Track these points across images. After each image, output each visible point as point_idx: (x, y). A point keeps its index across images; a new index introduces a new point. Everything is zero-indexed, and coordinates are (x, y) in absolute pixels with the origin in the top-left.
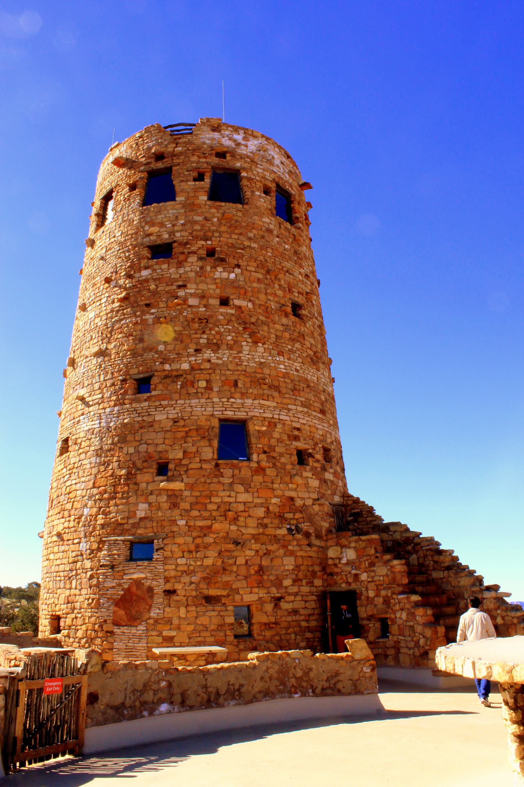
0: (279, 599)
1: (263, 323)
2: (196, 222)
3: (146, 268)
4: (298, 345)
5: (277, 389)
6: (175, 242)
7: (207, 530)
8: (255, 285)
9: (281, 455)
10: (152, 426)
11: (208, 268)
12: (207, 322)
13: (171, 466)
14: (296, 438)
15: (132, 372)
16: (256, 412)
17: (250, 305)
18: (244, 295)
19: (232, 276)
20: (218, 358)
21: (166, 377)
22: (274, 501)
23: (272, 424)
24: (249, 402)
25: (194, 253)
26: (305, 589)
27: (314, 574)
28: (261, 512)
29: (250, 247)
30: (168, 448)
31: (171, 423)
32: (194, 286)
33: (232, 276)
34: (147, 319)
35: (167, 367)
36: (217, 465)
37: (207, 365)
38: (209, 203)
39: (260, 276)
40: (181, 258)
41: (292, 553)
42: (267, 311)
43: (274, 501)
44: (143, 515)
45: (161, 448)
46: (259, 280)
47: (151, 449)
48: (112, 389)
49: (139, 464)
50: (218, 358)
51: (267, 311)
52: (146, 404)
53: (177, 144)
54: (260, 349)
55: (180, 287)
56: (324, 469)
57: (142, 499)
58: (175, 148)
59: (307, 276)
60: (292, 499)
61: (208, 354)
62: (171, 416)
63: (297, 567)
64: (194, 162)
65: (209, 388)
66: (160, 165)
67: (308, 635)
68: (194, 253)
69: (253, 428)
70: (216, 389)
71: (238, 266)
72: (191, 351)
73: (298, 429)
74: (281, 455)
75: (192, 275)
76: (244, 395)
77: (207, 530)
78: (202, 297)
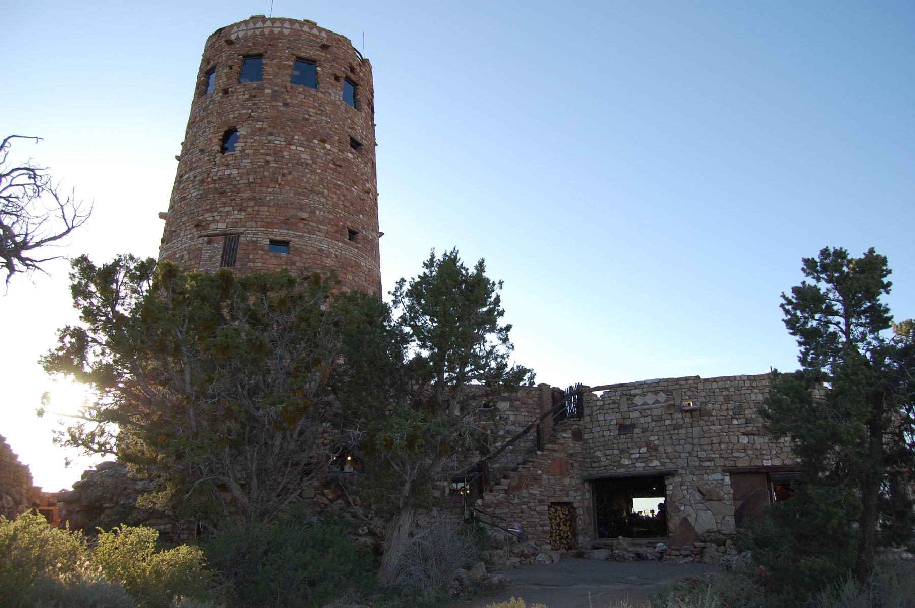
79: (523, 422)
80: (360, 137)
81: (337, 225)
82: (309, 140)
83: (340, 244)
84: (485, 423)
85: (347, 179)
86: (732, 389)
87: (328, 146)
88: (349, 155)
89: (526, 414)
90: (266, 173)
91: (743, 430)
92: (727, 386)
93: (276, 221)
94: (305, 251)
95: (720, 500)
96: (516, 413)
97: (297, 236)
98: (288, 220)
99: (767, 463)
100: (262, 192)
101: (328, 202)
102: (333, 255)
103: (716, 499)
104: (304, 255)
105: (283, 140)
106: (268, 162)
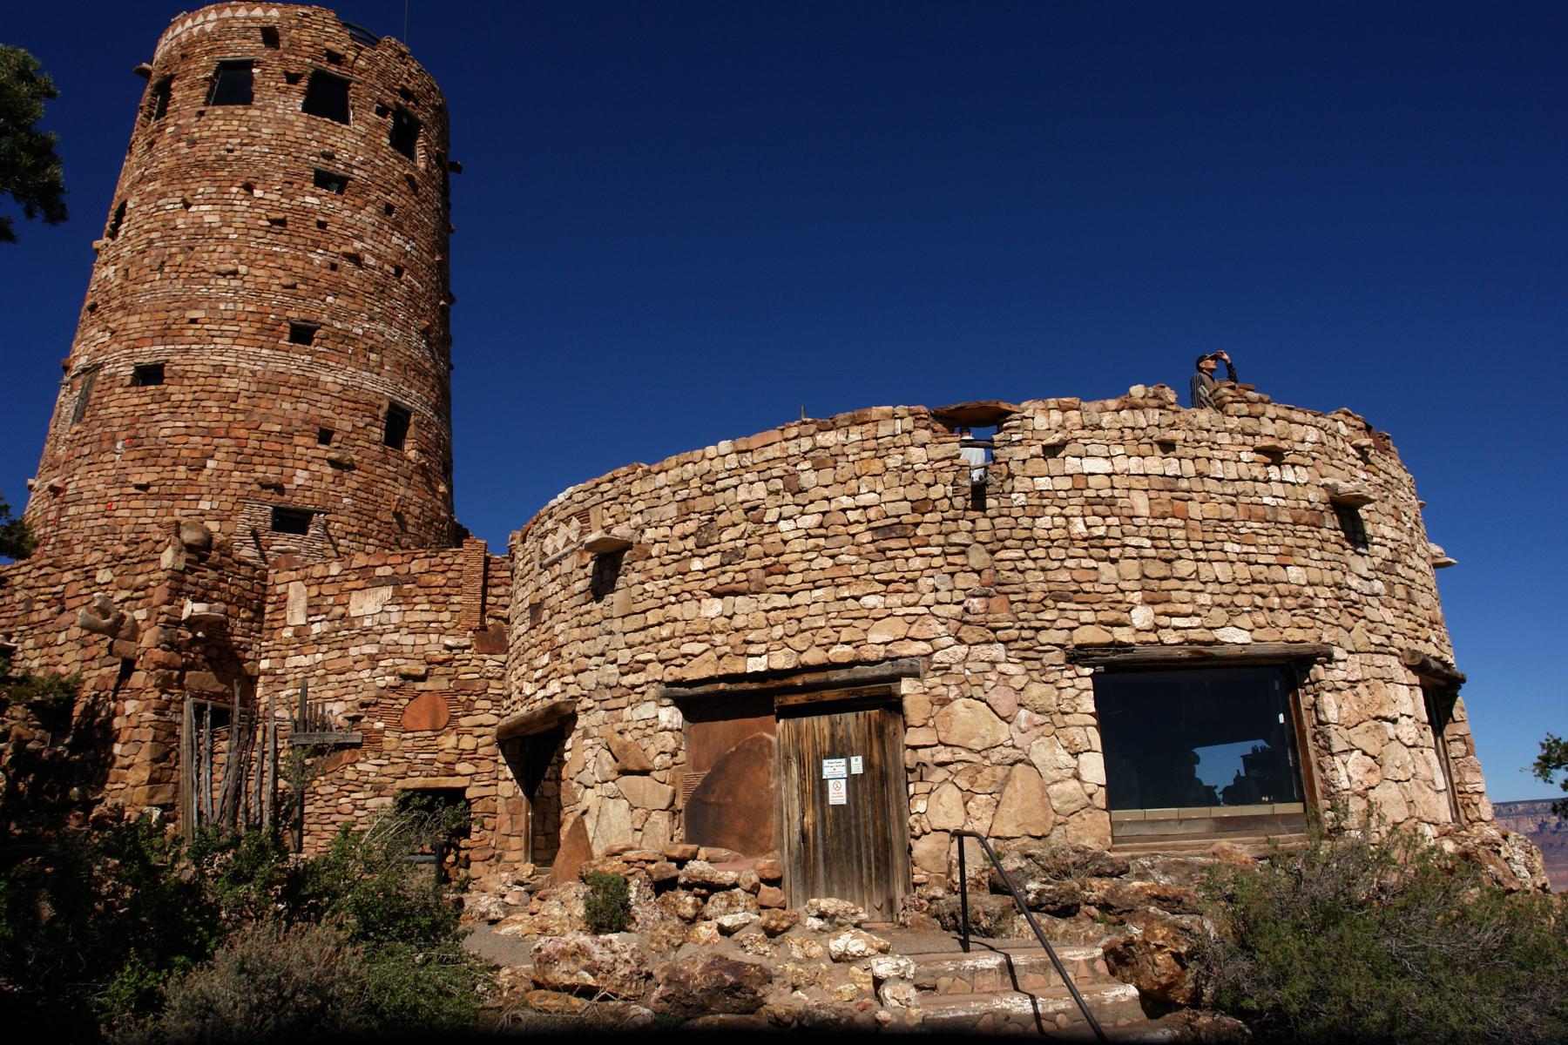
2: (375, 167)
3: (313, 195)
6: (352, 179)
10: (316, 386)
11: (386, 227)
12: (383, 292)
13: (337, 437)
15: (289, 314)
18: (414, 273)
20: (390, 334)
21: (336, 335)
25: (374, 203)
30: (335, 416)
31: (339, 388)
32: (371, 242)
34: (312, 260)
35: (338, 325)
36: (385, 452)
37: (381, 339)
38: (391, 149)
40: (358, 202)
44: (301, 482)
45: (325, 413)
47: (313, 411)
48: (259, 325)
49: (297, 423)
50: (390, 334)
52: (309, 358)
53: (359, 54)
55: (357, 237)
57: (302, 464)
58: (356, 58)
61: (381, 327)
62: (340, 381)
64: (378, 89)
65: (381, 365)
66: (333, 69)
68: (374, 203)
70: (387, 368)
71: (414, 239)
72: (365, 317)
75: (370, 228)
78: (378, 257)
79: (417, 625)
80: (342, 167)
81: (261, 321)
82: (221, 190)
83: (265, 351)
84: (346, 633)
85: (297, 240)
86: (695, 483)
87: (258, 193)
88: (309, 199)
89: (427, 607)
90: (146, 261)
91: (711, 584)
92: (686, 476)
93: (147, 334)
94: (189, 375)
95: (645, 772)
96: (404, 607)
97: (179, 351)
98: (170, 329)
99: (756, 665)
100: (134, 292)
101: (247, 285)
102: (246, 372)
103: (637, 769)
104: (186, 382)
105: (179, 200)
106: (151, 242)
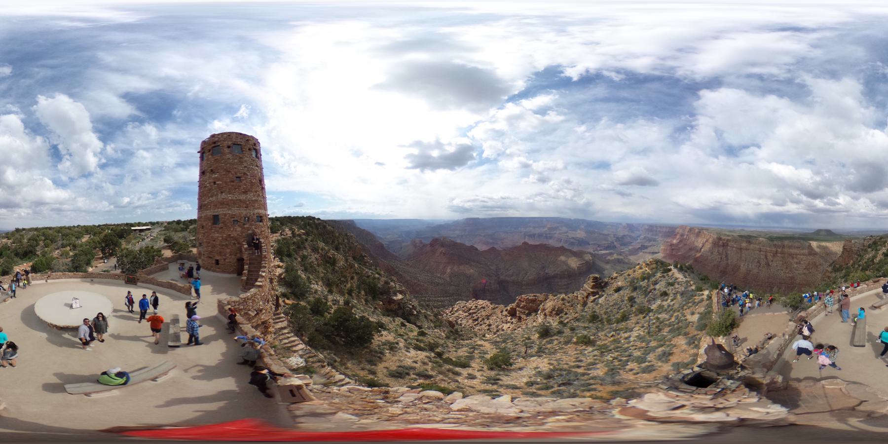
0: (226, 259)
1: (225, 186)
4: (237, 190)
5: (227, 204)
7: (209, 243)
8: (223, 176)
9: (228, 223)
14: (234, 218)
16: (221, 213)
17: (221, 182)
18: (219, 180)
19: (216, 176)
22: (225, 235)
23: (225, 215)
24: (219, 210)
26: (233, 257)
27: (237, 254)
28: (221, 239)
29: (222, 166)
33: (216, 176)
39: (224, 173)
41: (229, 249)
42: (226, 183)
43: (225, 235)
46: (224, 175)
51: (226, 183)
54: (224, 194)
56: (244, 224)
59: (245, 167)
60: (230, 235)
63: (231, 252)
65: (210, 208)
67: (235, 267)
69: (220, 217)
71: (218, 172)
73: (234, 215)
74: (228, 223)
76: (218, 208)
77: (209, 243)
